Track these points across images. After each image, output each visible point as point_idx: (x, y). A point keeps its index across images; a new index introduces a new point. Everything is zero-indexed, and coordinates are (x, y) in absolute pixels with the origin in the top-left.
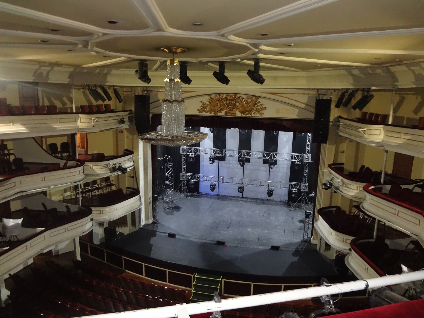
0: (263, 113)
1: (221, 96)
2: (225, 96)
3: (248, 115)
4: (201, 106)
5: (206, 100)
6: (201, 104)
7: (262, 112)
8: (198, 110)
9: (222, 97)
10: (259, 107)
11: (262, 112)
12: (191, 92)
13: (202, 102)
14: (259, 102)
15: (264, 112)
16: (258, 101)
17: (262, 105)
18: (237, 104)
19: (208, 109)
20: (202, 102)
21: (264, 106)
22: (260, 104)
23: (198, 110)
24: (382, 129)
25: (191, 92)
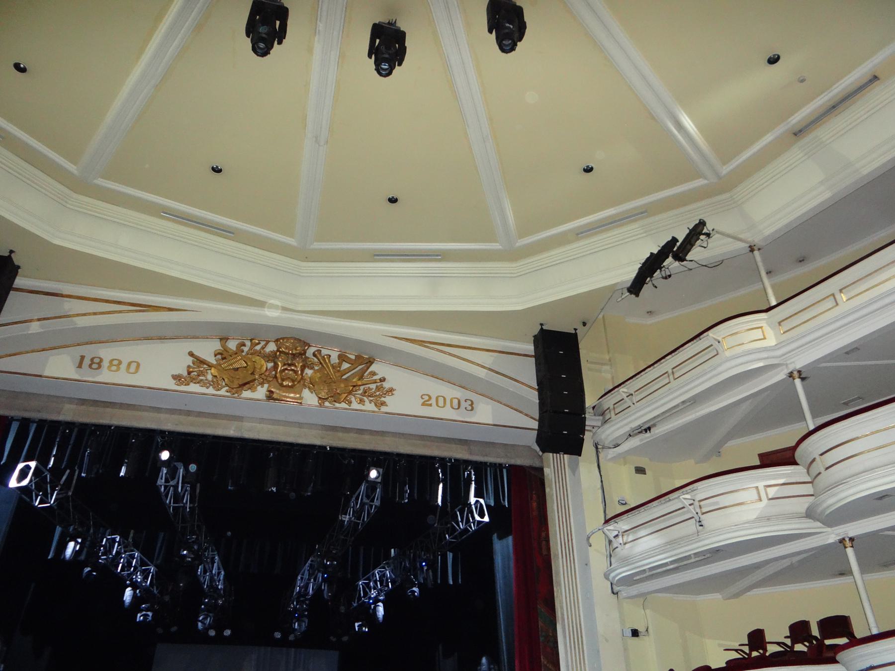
0: (383, 404)
1: (258, 348)
2: (272, 347)
3: (337, 405)
4: (189, 367)
5: (207, 350)
6: (189, 361)
7: (383, 399)
8: (175, 377)
9: (263, 348)
10: (373, 386)
11: (383, 399)
12: (170, 310)
13: (191, 354)
14: (374, 374)
15: (387, 399)
16: (370, 370)
17: (383, 380)
18: (309, 372)
19: (210, 377)
20: (191, 354)
21: (386, 385)
22: (375, 377)
23: (175, 377)
24: (763, 324)
25: (170, 310)
